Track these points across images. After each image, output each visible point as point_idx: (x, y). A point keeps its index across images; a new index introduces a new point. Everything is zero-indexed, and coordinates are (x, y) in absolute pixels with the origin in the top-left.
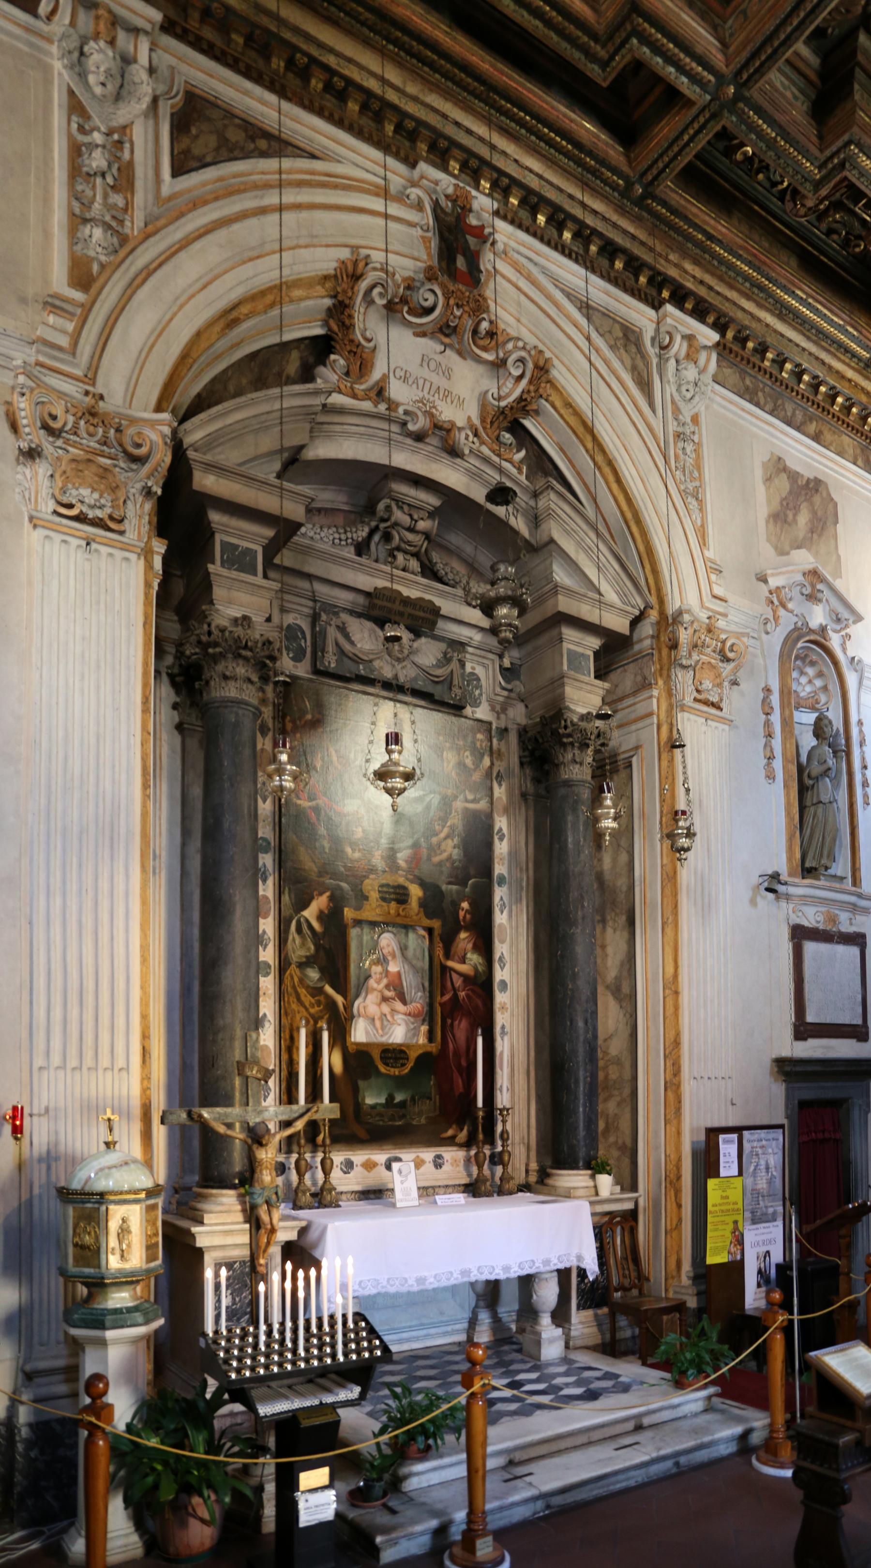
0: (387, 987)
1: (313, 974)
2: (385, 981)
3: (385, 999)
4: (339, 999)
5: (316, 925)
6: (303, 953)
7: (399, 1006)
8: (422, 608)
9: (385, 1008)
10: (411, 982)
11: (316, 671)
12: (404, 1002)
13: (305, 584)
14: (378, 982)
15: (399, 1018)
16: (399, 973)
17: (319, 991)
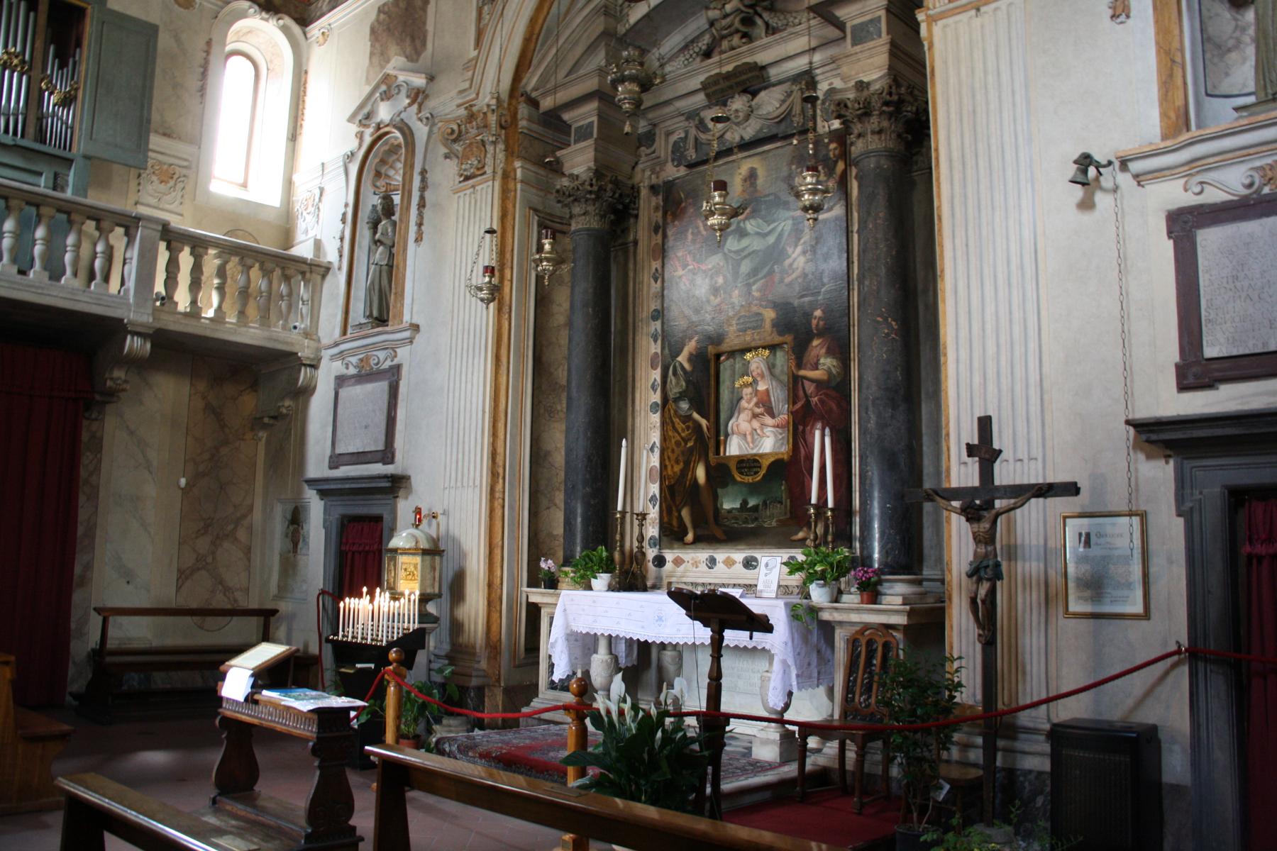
0: (757, 405)
1: (684, 405)
2: (755, 400)
3: (755, 416)
4: (704, 422)
5: (687, 366)
6: (676, 390)
7: (768, 420)
8: (742, 73)
9: (756, 424)
10: (779, 397)
11: (690, 166)
12: (773, 416)
13: (668, 110)
14: (749, 402)
15: (768, 430)
16: (767, 391)
17: (689, 418)
